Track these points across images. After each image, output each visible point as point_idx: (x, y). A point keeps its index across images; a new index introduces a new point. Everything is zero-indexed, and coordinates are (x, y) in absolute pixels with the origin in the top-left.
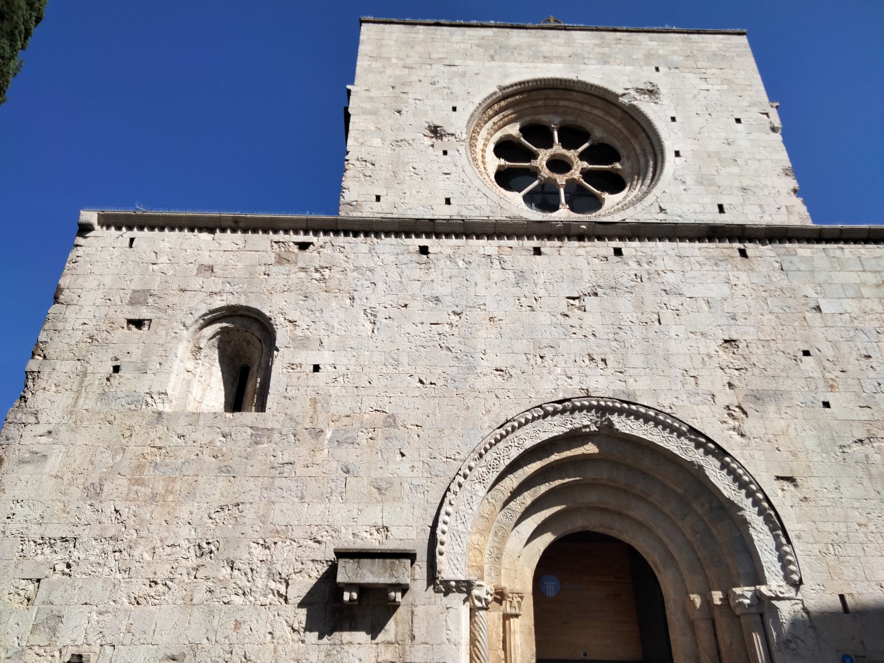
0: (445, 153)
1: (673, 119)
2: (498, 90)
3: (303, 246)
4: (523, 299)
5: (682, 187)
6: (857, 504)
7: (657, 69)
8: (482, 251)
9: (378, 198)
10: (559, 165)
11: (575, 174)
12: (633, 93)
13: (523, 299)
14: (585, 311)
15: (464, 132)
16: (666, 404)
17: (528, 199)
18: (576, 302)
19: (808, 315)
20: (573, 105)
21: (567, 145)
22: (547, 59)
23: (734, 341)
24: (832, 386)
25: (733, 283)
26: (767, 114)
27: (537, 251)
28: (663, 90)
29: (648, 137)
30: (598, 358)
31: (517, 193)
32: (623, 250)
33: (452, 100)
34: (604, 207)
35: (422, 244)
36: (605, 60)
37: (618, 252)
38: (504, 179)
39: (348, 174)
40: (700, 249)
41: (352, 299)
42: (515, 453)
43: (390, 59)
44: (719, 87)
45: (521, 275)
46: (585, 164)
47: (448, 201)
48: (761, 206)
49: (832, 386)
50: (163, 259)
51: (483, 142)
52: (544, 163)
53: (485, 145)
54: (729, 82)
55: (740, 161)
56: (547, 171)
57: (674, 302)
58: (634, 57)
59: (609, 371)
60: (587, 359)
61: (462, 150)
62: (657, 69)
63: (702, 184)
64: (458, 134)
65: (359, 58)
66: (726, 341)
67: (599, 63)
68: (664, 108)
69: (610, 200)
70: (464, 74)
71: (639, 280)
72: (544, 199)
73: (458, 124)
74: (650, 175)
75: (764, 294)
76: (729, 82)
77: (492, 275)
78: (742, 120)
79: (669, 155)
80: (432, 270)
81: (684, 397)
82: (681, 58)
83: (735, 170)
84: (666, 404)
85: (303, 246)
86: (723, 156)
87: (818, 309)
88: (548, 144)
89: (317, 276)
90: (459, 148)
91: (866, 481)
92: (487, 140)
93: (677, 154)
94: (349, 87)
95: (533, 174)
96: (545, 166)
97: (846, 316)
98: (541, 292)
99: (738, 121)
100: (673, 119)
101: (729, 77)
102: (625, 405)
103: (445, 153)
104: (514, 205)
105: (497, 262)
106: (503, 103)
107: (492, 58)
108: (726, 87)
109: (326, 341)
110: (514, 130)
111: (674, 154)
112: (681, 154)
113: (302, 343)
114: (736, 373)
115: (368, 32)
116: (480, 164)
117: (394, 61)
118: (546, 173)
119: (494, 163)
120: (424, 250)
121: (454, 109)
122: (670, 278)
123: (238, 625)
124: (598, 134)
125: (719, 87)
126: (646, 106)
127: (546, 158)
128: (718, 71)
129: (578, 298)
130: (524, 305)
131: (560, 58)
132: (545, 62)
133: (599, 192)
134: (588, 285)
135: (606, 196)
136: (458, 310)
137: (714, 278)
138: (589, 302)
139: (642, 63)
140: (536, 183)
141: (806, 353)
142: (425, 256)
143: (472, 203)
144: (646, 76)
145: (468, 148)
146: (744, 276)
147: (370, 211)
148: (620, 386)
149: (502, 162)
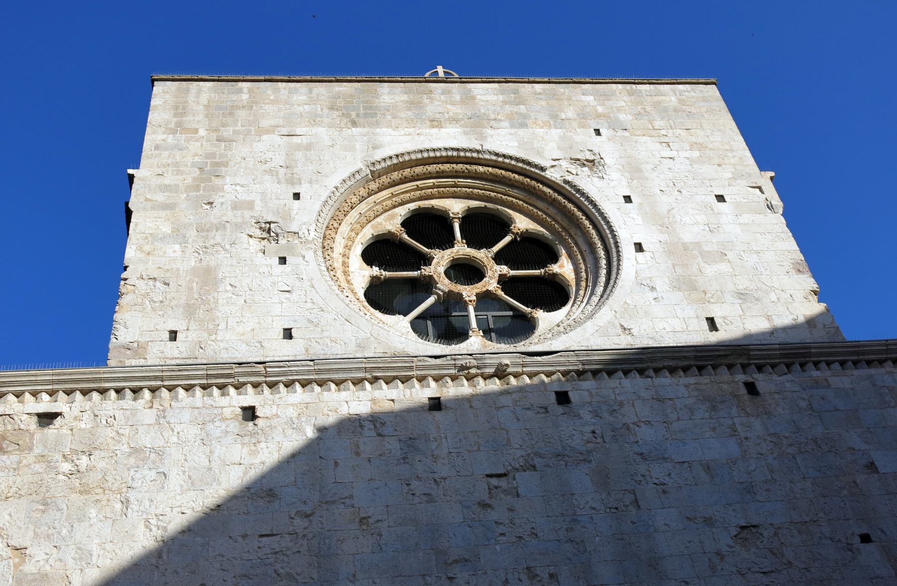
0: (283, 260)
2: (364, 168)
3: (47, 418)
4: (415, 484)
5: (651, 295)
7: (598, 132)
9: (173, 335)
10: (466, 271)
11: (491, 284)
12: (565, 164)
13: (415, 484)
14: (518, 495)
15: (312, 228)
17: (418, 327)
18: (503, 483)
19: (860, 478)
22: (436, 123)
23: (754, 526)
25: (743, 435)
26: (760, 188)
28: (608, 160)
31: (401, 317)
32: (571, 394)
33: (293, 184)
34: (538, 332)
35: (246, 404)
36: (520, 122)
38: (380, 297)
39: (123, 301)
40: (687, 386)
41: (126, 503)
43: (196, 131)
44: (687, 154)
46: (504, 269)
47: (288, 334)
51: (343, 242)
52: (442, 270)
53: (348, 247)
54: (701, 147)
55: (731, 255)
56: (447, 281)
57: (658, 472)
58: (563, 116)
60: (524, 577)
61: (310, 255)
62: (598, 132)
63: (679, 289)
64: (303, 231)
65: (149, 129)
66: (743, 528)
67: (512, 126)
68: (612, 184)
69: (545, 319)
70: (308, 147)
71: (599, 440)
72: (445, 325)
73: (305, 218)
74: (602, 279)
75: (790, 450)
76: (701, 147)
77: (362, 447)
78: (726, 198)
80: (263, 445)
82: (630, 117)
83: (724, 267)
85: (47, 418)
86: (706, 248)
87: (871, 467)
88: (447, 242)
89: (66, 467)
90: (303, 253)
92: (352, 240)
93: (639, 247)
94: (130, 171)
96: (443, 275)
98: (443, 470)
99: (720, 198)
100: (628, 199)
101: (701, 140)
103: (283, 260)
104: (396, 333)
107: (354, 124)
108: (696, 154)
112: (644, 247)
114: (765, 580)
115: (164, 94)
116: (339, 274)
117: (202, 132)
118: (445, 284)
120: (250, 413)
122: (645, 434)
124: (522, 223)
125: (687, 154)
126: (587, 182)
128: (684, 133)
129: (505, 475)
130: (417, 493)
131: (454, 120)
132: (433, 127)
133: (529, 310)
134: (520, 453)
135: (541, 315)
136: (308, 509)
137: (714, 429)
138: (526, 481)
139: (575, 124)
140: (431, 300)
141: (866, 539)
142: (251, 424)
143: (326, 334)
144: (585, 141)
145: (320, 253)
146: (757, 424)
147: (161, 354)
149: (375, 271)
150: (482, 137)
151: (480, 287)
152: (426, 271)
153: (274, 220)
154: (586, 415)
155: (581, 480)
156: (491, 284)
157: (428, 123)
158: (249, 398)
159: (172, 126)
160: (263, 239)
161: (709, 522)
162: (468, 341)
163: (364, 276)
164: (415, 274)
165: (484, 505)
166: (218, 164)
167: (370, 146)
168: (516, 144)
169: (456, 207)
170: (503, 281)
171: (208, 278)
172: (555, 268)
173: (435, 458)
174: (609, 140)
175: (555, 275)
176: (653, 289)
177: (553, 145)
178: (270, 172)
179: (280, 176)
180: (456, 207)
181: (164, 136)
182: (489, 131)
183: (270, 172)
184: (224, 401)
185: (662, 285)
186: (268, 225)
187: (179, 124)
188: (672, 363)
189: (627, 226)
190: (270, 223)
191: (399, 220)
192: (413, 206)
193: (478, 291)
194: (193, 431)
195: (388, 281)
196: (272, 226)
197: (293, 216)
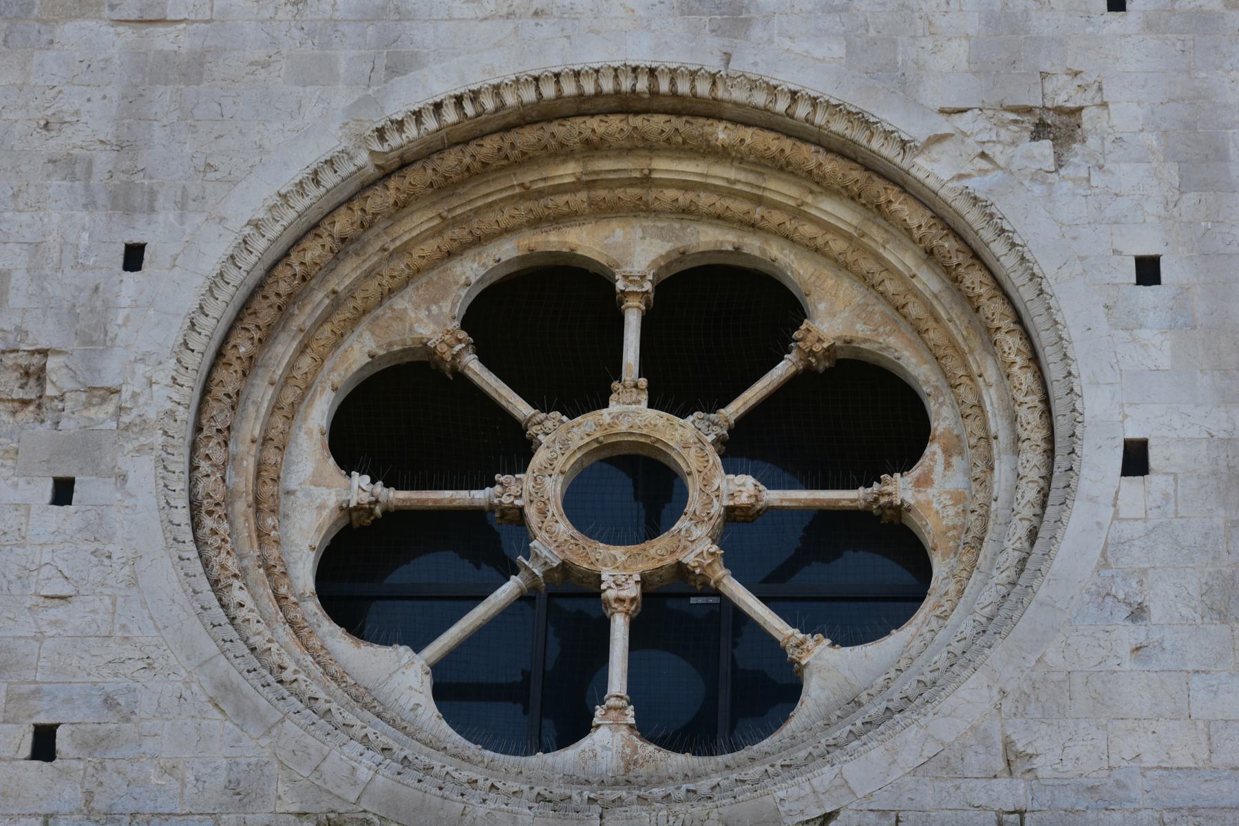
0: (63, 492)
1: (1148, 271)
15: (163, 377)
20: (722, 173)
21: (669, 394)
29: (1035, 358)
31: (404, 652)
33: (129, 211)
38: (364, 579)
46: (744, 488)
52: (554, 488)
56: (564, 528)
70: (193, 69)
79: (1100, 462)
88: (585, 390)
93: (1136, 459)
95: (492, 542)
96: (555, 508)
100: (1148, 271)
103: (63, 492)
106: (379, 200)
110: (430, 319)
111: (1116, 460)
119: (321, 493)
121: (134, 257)
127: (565, 462)
149: (361, 488)
151: (657, 553)
152: (505, 491)
153: (55, 343)
156: (692, 542)
160: (25, 403)
162: (585, 743)
163: (321, 508)
164: (479, 497)
167: (382, 62)
168: (838, 50)
169: (635, 254)
170: (736, 523)
172: (900, 488)
174: (1150, 26)
175: (899, 510)
176: (1138, 613)
177: (957, 53)
178: (68, 166)
179: (94, 181)
180: (635, 254)
183: (68, 166)
185: (1171, 597)
186: (36, 360)
190: (44, 353)
191: (454, 304)
192: (507, 250)
193: (650, 566)
195: (397, 517)
196: (52, 363)
197: (113, 330)
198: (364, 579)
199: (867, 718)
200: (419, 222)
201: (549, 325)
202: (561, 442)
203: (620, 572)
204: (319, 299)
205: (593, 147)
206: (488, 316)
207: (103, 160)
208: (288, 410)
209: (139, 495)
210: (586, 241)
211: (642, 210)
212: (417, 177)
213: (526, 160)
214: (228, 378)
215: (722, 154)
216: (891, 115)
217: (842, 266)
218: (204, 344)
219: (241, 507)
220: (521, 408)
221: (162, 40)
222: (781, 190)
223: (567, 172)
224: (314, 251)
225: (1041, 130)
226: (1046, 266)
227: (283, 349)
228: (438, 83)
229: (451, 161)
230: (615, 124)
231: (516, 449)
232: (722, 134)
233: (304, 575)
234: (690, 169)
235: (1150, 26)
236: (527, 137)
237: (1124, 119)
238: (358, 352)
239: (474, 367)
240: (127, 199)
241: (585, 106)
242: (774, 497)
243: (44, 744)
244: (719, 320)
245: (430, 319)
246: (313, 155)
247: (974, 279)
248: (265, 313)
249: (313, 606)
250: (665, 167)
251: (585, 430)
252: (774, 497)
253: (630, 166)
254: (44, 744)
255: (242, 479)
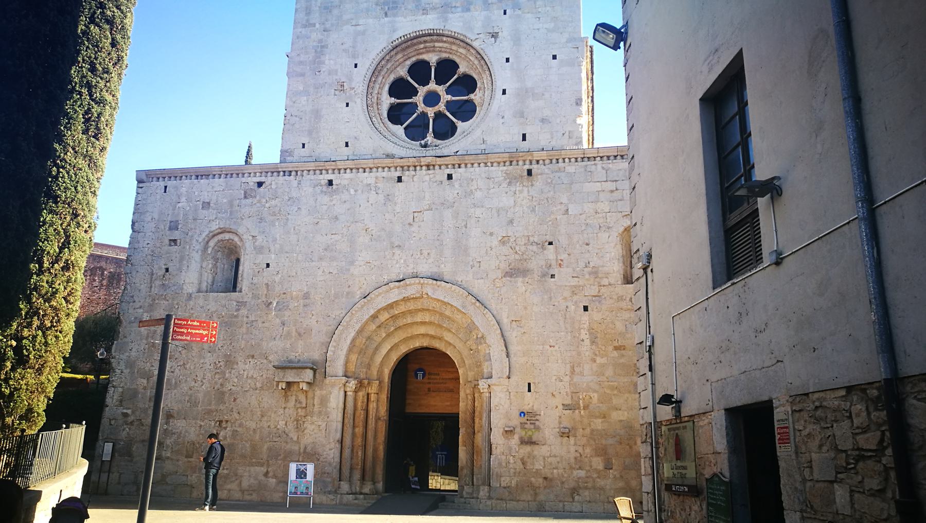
0: (347, 105)
1: (508, 60)
3: (260, 184)
4: (387, 215)
5: (502, 121)
6: (552, 335)
7: (505, 13)
8: (365, 182)
9: (304, 145)
13: (387, 215)
16: (460, 280)
20: (445, 45)
21: (439, 83)
22: (425, 11)
24: (560, 265)
27: (400, 179)
30: (425, 253)
37: (450, 177)
38: (395, 115)
42: (372, 312)
43: (314, 25)
45: (388, 198)
46: (449, 97)
48: (552, 134)
49: (560, 265)
50: (183, 199)
52: (421, 99)
54: (554, 19)
56: (423, 105)
57: (478, 212)
59: (430, 261)
67: (463, 11)
70: (363, 33)
76: (554, 19)
81: (471, 276)
84: (460, 280)
85: (260, 184)
88: (425, 82)
91: (562, 323)
93: (504, 92)
97: (584, 216)
100: (508, 60)
102: (435, 282)
103: (347, 105)
105: (373, 189)
106: (393, 53)
109: (272, 249)
110: (403, 72)
113: (259, 250)
117: (317, 26)
118: (421, 107)
120: (330, 183)
121: (356, 66)
123: (235, 400)
138: (427, 215)
141: (550, 243)
148: (435, 270)
149: (393, 100)
150: (446, 20)
151: (436, 109)
154: (457, 186)
155: (448, 213)
156: (441, 107)
157: (421, 12)
158: (330, 176)
159: (304, 22)
161: (491, 234)
165: (410, 224)
166: (322, 47)
168: (461, 24)
169: (433, 59)
170: (449, 104)
171: (317, 114)
172: (472, 96)
173: (396, 204)
174: (510, 17)
177: (480, 23)
180: (433, 59)
181: (300, 30)
182: (450, 15)
184: (321, 177)
187: (307, 21)
188: (499, 160)
189: (503, 77)
192: (414, 59)
194: (311, 190)
195: (398, 104)
198: (395, 115)
199: (466, 134)
200: (400, 56)
201: (420, 71)
202: (422, 91)
203: (431, 112)
204: (385, 70)
205: (425, 42)
206: (412, 70)
207: (351, 49)
208: (381, 88)
209: (359, 105)
210: (425, 57)
211: (434, 51)
212: (399, 49)
213: (415, 45)
214: (371, 84)
215: (445, 42)
216: (469, 35)
217: (464, 59)
218: (367, 79)
219: (375, 105)
220: (416, 85)
221: (359, 28)
222: (454, 47)
223: (422, 46)
224: (383, 62)
225: (493, 36)
226: (492, 60)
227: (380, 78)
228: (400, 33)
229: (404, 46)
230: (428, 38)
231: (415, 92)
232: (445, 39)
233: (385, 114)
234: (440, 45)
235: (510, 17)
236: (415, 41)
237: (504, 34)
238: (392, 78)
239: (409, 79)
240: (354, 56)
241: (424, 35)
242: (454, 98)
243: (347, 145)
244: (447, 68)
245: (403, 72)
246: (381, 47)
247: (482, 62)
248: (377, 73)
249: (387, 119)
250: (437, 44)
251: (426, 88)
252: (454, 98)
253: (431, 44)
254: (347, 145)
255: (375, 100)
